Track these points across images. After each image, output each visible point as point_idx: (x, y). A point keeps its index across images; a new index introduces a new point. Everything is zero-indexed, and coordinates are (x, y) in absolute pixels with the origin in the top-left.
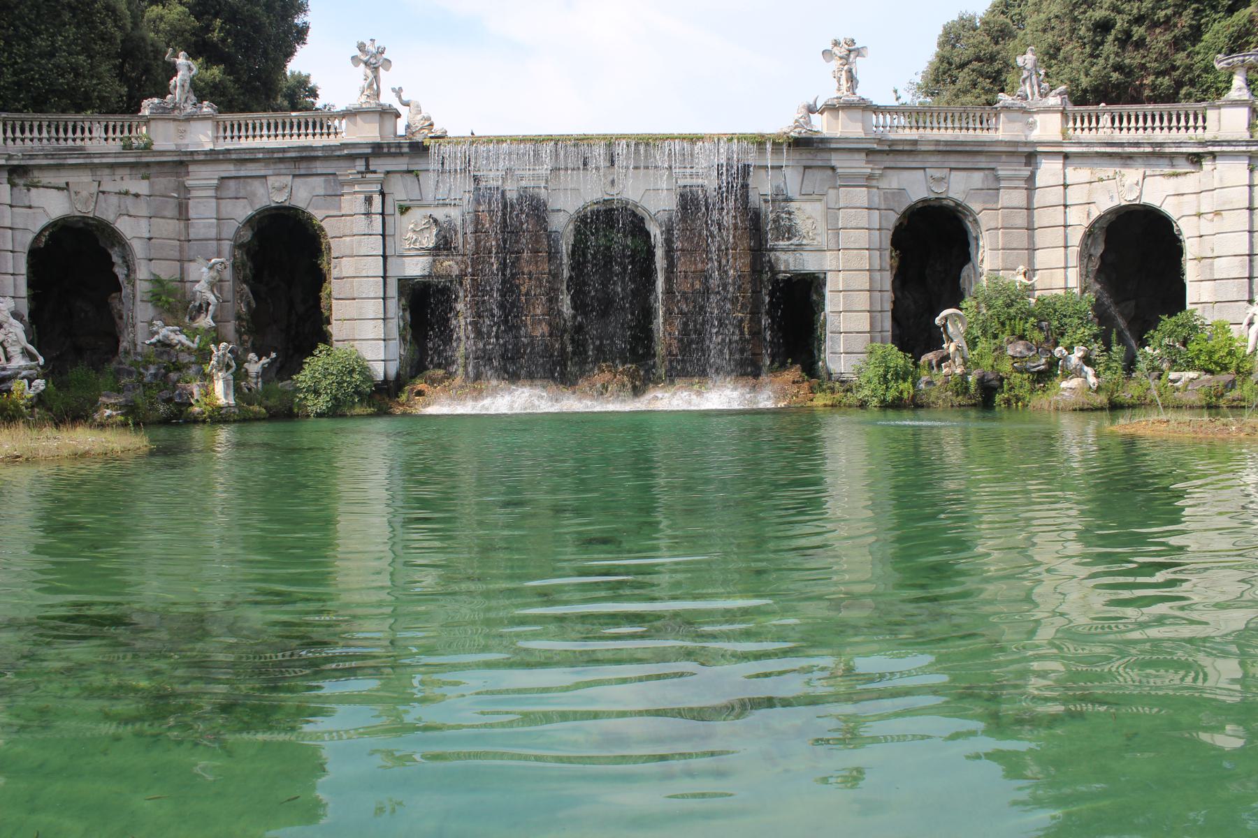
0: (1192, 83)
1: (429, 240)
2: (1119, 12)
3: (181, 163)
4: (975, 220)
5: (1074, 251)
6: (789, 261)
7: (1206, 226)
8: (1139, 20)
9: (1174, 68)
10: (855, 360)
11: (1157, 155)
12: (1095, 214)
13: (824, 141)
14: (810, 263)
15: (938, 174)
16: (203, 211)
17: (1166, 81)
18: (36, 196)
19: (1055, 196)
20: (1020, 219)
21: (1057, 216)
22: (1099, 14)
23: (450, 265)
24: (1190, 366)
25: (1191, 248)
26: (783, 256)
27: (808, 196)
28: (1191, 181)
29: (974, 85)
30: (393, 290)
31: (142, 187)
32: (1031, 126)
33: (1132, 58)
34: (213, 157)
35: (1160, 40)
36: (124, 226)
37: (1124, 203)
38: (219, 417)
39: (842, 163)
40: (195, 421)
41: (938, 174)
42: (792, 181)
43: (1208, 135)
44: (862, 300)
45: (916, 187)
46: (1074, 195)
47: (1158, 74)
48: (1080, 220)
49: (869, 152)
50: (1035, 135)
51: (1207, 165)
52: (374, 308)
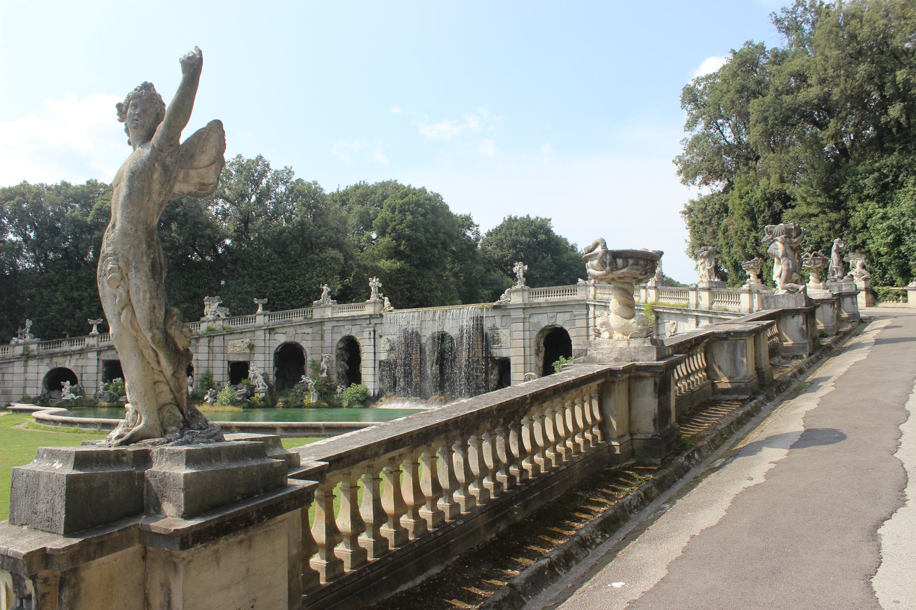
1: (388, 348)
3: (322, 322)
15: (551, 315)
16: (328, 337)
18: (277, 336)
20: (584, 332)
26: (495, 351)
27: (505, 327)
30: (377, 365)
31: (309, 331)
34: (330, 320)
36: (303, 344)
38: (310, 406)
39: (514, 314)
40: (305, 407)
41: (551, 315)
52: (371, 371)
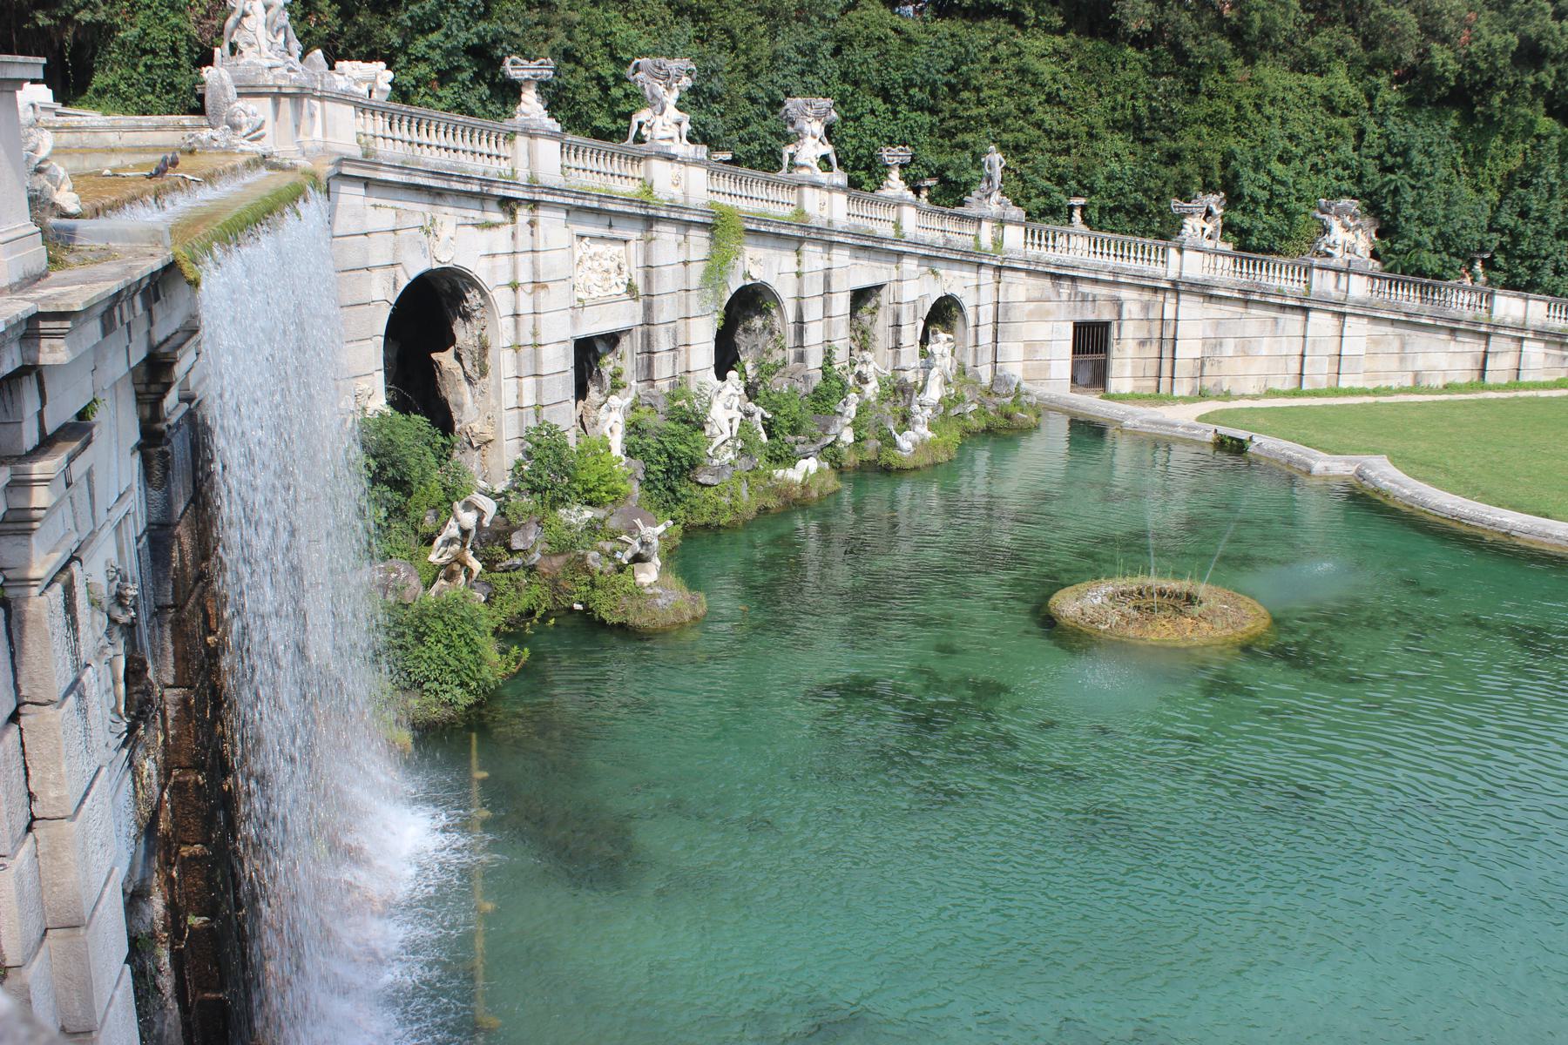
12: (404, 283)
37: (436, 266)
51: (523, 214)
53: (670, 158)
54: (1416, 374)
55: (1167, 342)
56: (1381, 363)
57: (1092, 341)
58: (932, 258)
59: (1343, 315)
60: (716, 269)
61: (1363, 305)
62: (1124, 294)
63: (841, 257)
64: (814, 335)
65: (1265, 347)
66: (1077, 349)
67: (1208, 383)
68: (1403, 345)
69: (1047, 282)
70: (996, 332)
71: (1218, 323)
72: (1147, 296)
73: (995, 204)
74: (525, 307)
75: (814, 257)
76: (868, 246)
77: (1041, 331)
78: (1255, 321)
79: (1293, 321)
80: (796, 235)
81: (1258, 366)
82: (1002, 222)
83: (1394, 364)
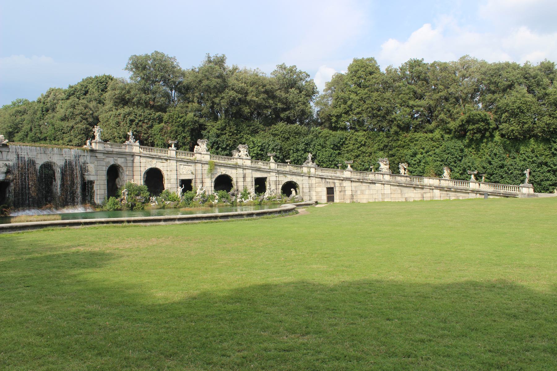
0: (151, 137)
2: (136, 118)
4: (122, 169)
5: (142, 176)
6: (87, 178)
7: (169, 173)
8: (140, 121)
9: (148, 133)
10: (102, 200)
11: (159, 158)
13: (96, 150)
14: (92, 178)
15: (116, 158)
17: (146, 136)
19: (138, 164)
21: (139, 169)
22: (132, 118)
23: (10, 177)
24: (169, 200)
25: (165, 177)
28: (165, 164)
29: (81, 121)
32: (133, 149)
33: (139, 129)
35: (145, 126)
41: (116, 158)
42: (88, 159)
43: (169, 156)
44: (102, 187)
45: (111, 161)
46: (142, 165)
47: (145, 134)
48: (143, 170)
49: (104, 153)
50: (134, 151)
51: (169, 161)
53: (201, 154)
54: (406, 198)
55: (343, 191)
56: (395, 196)
57: (330, 191)
58: (278, 172)
59: (384, 184)
60: (211, 171)
61: (389, 182)
62: (336, 181)
63: (248, 172)
64: (241, 184)
65: (367, 192)
66: (328, 193)
67: (355, 200)
68: (401, 191)
69: (320, 179)
70: (310, 190)
71: (356, 187)
72: (341, 181)
73: (310, 164)
74: (169, 173)
75: (240, 171)
76: (259, 170)
77: (319, 189)
78: (364, 186)
79: (372, 186)
80: (236, 167)
81: (366, 197)
82: (310, 167)
83: (400, 196)
